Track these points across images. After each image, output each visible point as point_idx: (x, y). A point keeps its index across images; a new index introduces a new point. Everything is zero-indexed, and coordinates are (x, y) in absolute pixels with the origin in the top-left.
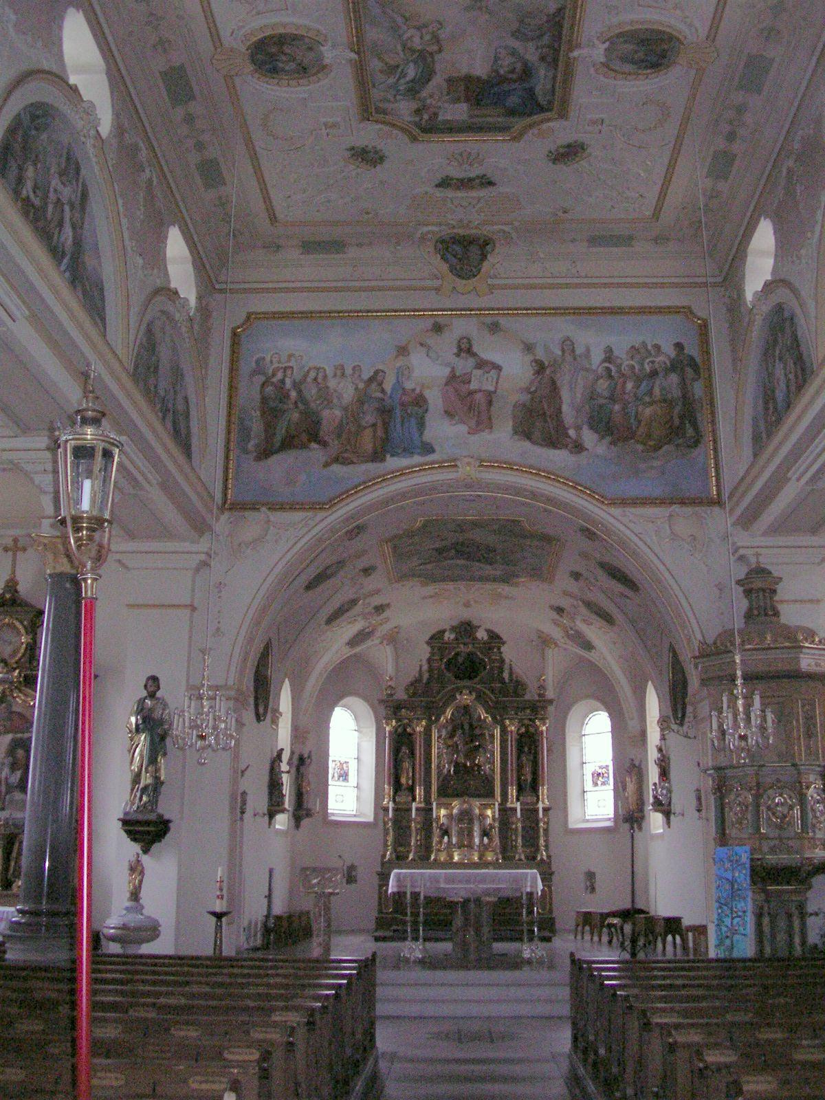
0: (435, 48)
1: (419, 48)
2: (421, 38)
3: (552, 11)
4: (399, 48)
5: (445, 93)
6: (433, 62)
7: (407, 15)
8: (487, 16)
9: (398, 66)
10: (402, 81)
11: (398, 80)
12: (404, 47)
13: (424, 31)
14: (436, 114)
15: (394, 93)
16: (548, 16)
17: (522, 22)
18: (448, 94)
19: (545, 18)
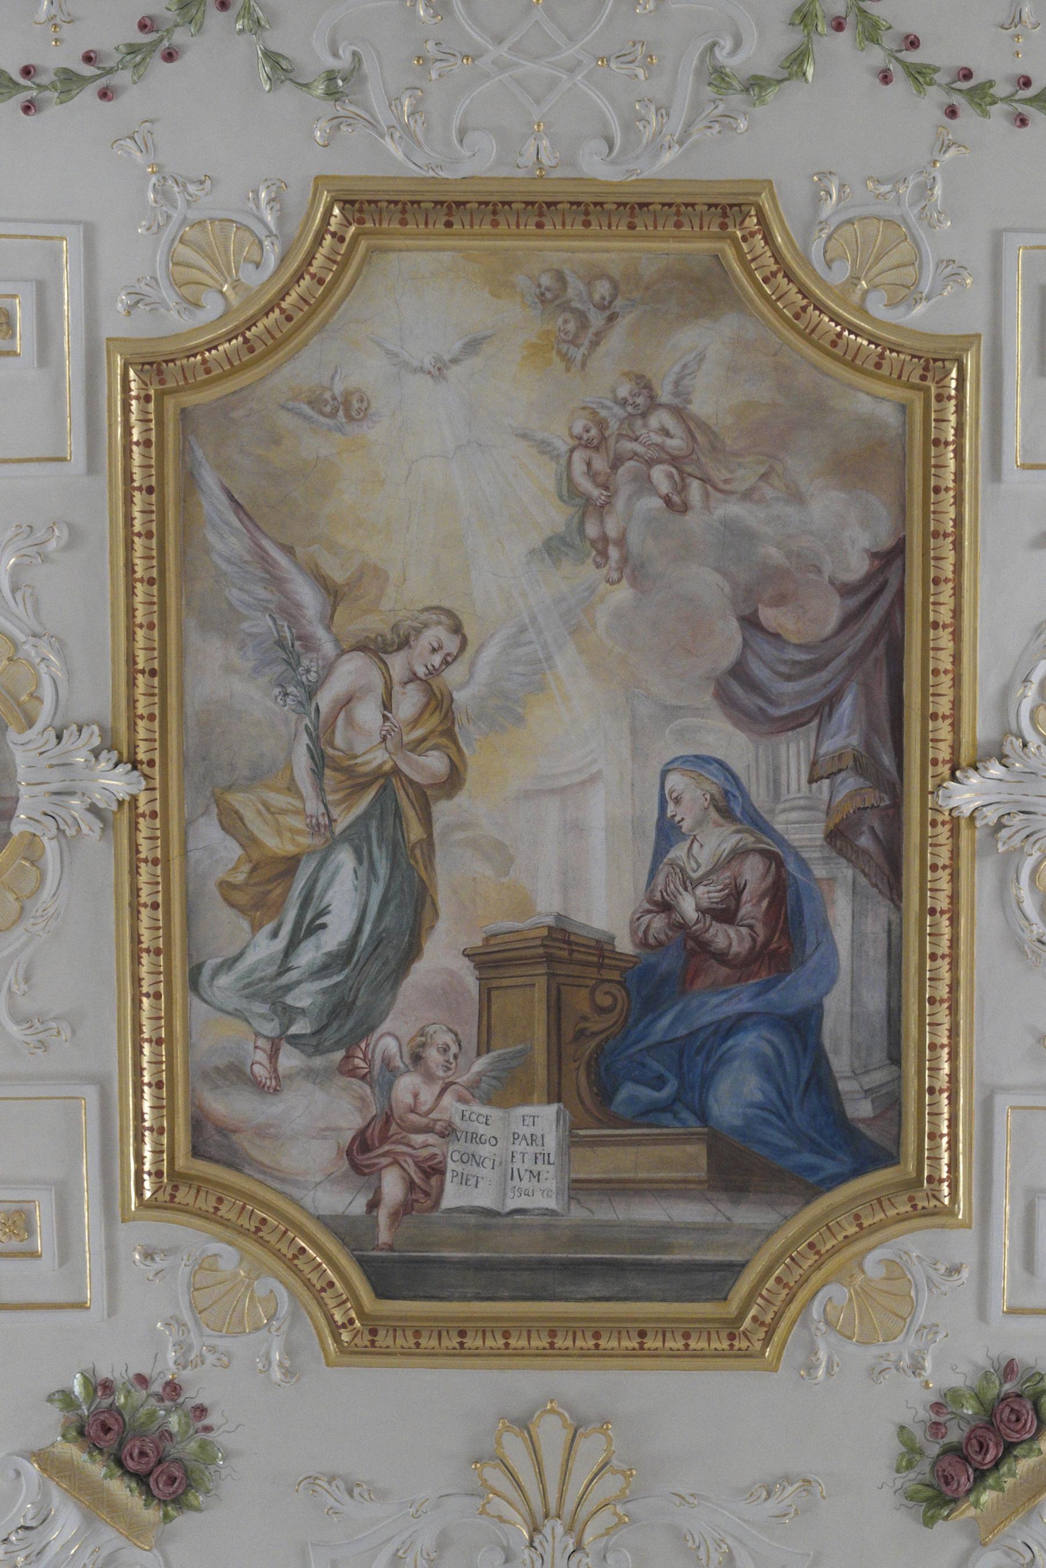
0: (435, 763)
1: (378, 758)
2: (387, 705)
3: (857, 567)
4: (302, 763)
5: (470, 1032)
6: (429, 843)
7: (338, 576)
8: (623, 594)
9: (291, 865)
10: (308, 956)
11: (292, 945)
12: (320, 761)
13: (397, 664)
14: (434, 1170)
15: (270, 1028)
16: (846, 590)
17: (750, 622)
18: (484, 1047)
19: (834, 611)
